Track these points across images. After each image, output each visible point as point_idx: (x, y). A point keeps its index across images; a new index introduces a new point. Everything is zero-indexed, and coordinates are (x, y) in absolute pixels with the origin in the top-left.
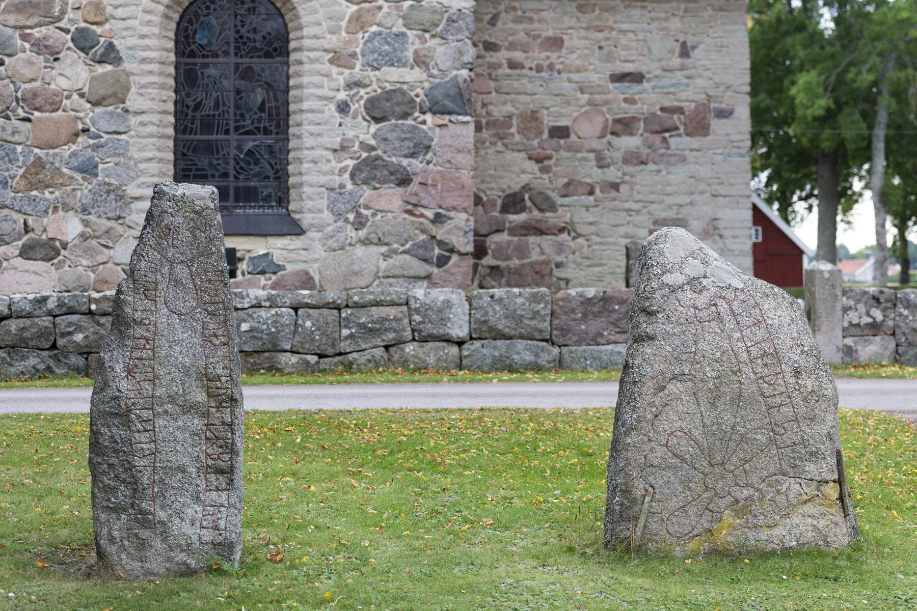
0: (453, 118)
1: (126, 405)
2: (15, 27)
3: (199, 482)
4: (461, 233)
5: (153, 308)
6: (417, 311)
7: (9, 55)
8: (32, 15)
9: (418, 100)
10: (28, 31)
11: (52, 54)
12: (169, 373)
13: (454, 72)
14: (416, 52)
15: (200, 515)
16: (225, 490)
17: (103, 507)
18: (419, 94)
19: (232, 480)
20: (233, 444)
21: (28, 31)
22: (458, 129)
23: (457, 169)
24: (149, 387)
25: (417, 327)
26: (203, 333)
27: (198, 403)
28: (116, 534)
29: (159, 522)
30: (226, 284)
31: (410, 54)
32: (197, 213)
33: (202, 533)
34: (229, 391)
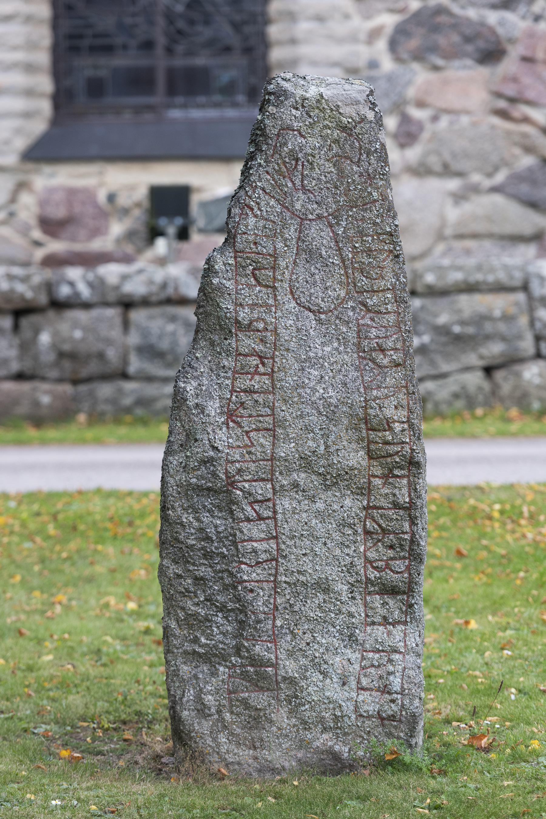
1: (227, 473)
3: (353, 609)
5: (271, 302)
12: (301, 416)
15: (357, 667)
16: (399, 622)
17: (186, 653)
19: (411, 606)
20: (412, 541)
24: (265, 441)
26: (358, 345)
27: (352, 469)
28: (209, 699)
29: (285, 679)
30: (397, 256)
32: (344, 128)
33: (361, 698)
34: (407, 448)
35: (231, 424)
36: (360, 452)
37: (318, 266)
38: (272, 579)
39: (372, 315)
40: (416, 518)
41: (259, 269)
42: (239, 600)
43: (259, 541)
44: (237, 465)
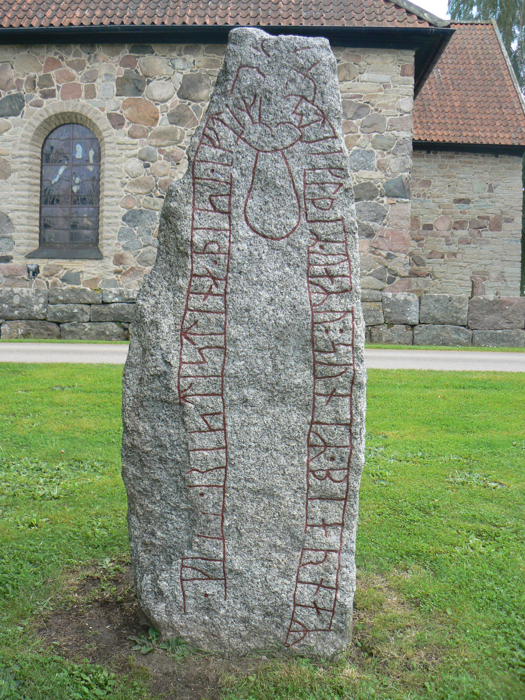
0: (399, 199)
2: (156, 146)
4: (402, 265)
6: (388, 306)
7: (153, 162)
8: (165, 139)
9: (379, 189)
10: (163, 148)
11: (175, 161)
13: (400, 174)
14: (379, 162)
18: (380, 186)
21: (163, 148)
22: (402, 206)
23: (401, 229)
25: (388, 315)
27: (298, 386)
31: (375, 163)
35: (185, 340)
36: (307, 372)
37: (272, 195)
38: (222, 484)
39: (322, 243)
40: (356, 434)
41: (217, 196)
43: (210, 450)
44: (189, 379)
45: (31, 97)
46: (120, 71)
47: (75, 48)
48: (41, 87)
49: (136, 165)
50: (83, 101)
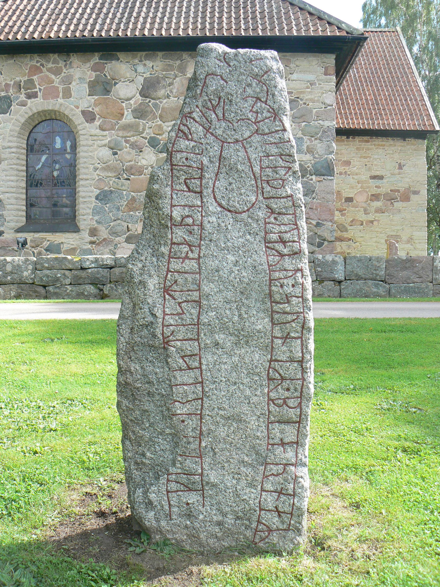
0: (325, 177)
2: (122, 137)
4: (329, 232)
6: (319, 265)
7: (120, 150)
8: (130, 131)
9: (309, 169)
10: (128, 139)
11: (139, 149)
13: (326, 156)
14: (308, 147)
21: (128, 139)
22: (327, 183)
23: (327, 201)
25: (319, 273)
27: (259, 332)
31: (305, 147)
35: (167, 296)
36: (266, 319)
37: (235, 177)
38: (199, 412)
39: (276, 216)
40: (307, 368)
41: (190, 179)
42: (174, 428)
43: (189, 385)
44: (171, 328)
45: (18, 98)
46: (91, 75)
47: (54, 57)
48: (26, 89)
49: (106, 153)
50: (61, 100)
